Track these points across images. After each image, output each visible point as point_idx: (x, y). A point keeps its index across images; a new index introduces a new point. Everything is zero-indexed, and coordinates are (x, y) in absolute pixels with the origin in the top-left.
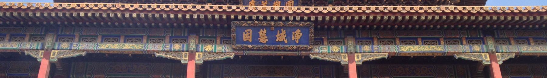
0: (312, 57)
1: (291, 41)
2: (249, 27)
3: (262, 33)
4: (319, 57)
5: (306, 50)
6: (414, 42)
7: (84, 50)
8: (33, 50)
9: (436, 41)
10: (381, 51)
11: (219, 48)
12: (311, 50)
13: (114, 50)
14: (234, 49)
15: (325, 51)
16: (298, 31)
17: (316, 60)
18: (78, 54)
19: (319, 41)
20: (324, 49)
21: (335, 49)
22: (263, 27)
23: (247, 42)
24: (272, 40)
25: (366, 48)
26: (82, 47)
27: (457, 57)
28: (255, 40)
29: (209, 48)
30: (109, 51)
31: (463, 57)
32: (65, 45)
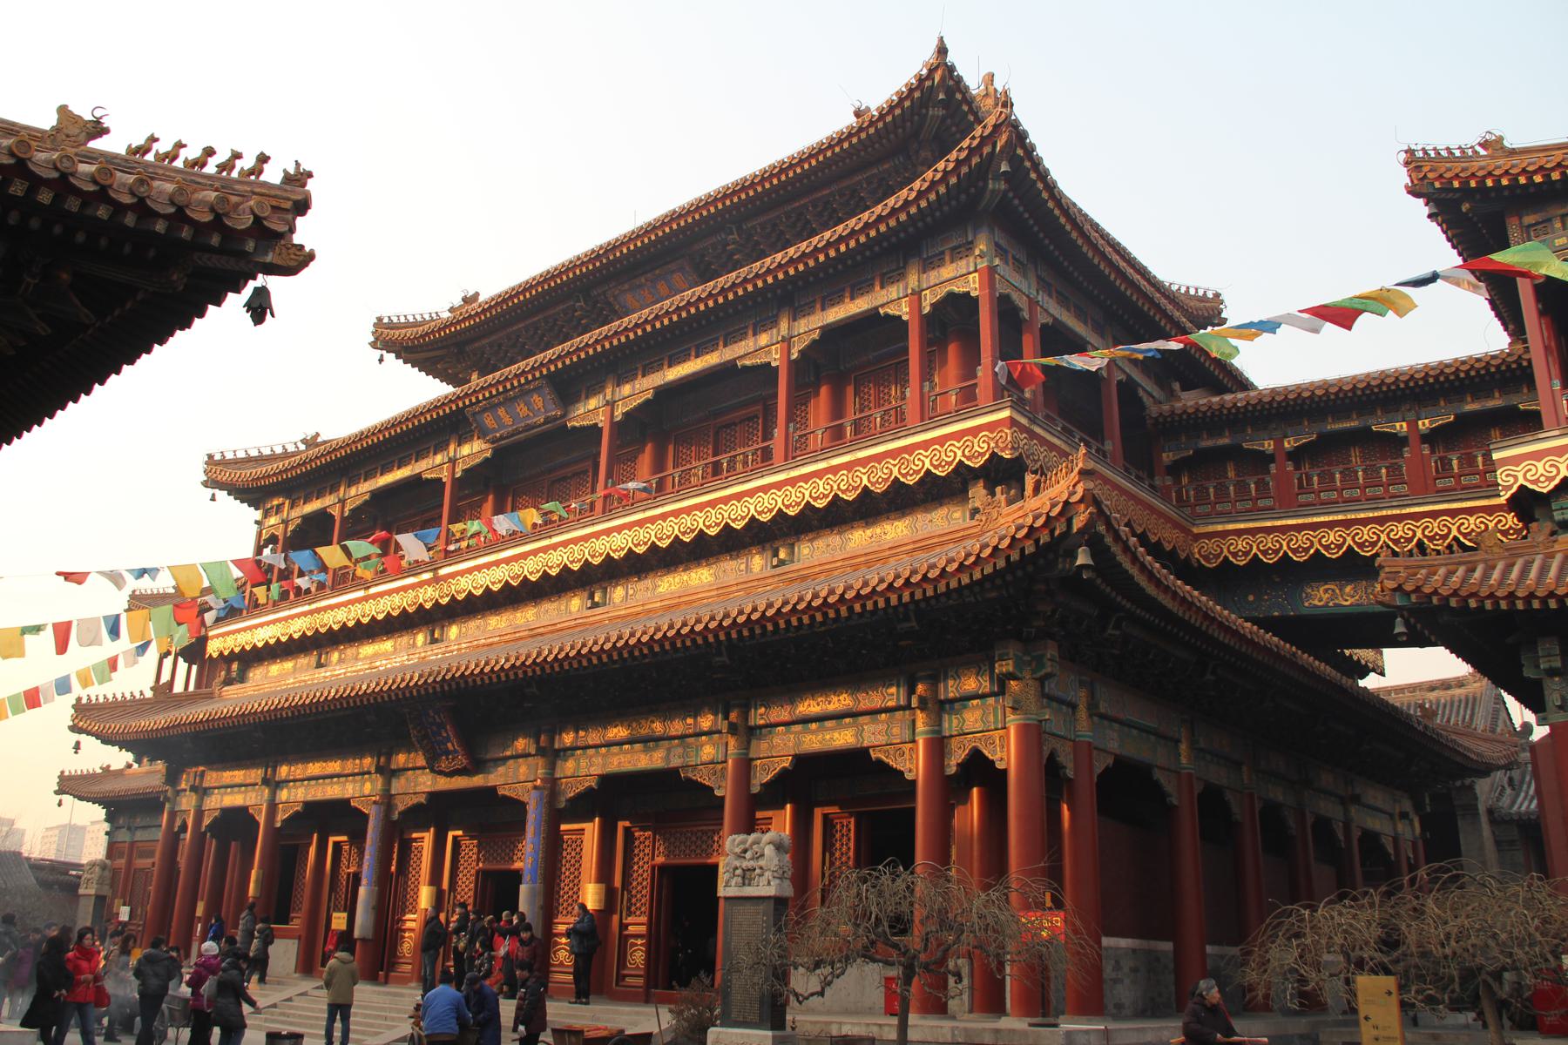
1: (537, 410)
2: (485, 410)
5: (555, 418)
6: (682, 358)
9: (710, 347)
10: (635, 392)
16: (535, 396)
17: (574, 428)
20: (581, 409)
22: (499, 404)
23: (494, 430)
24: (515, 417)
25: (627, 389)
28: (502, 426)
29: (466, 450)
31: (748, 362)
32: (353, 491)
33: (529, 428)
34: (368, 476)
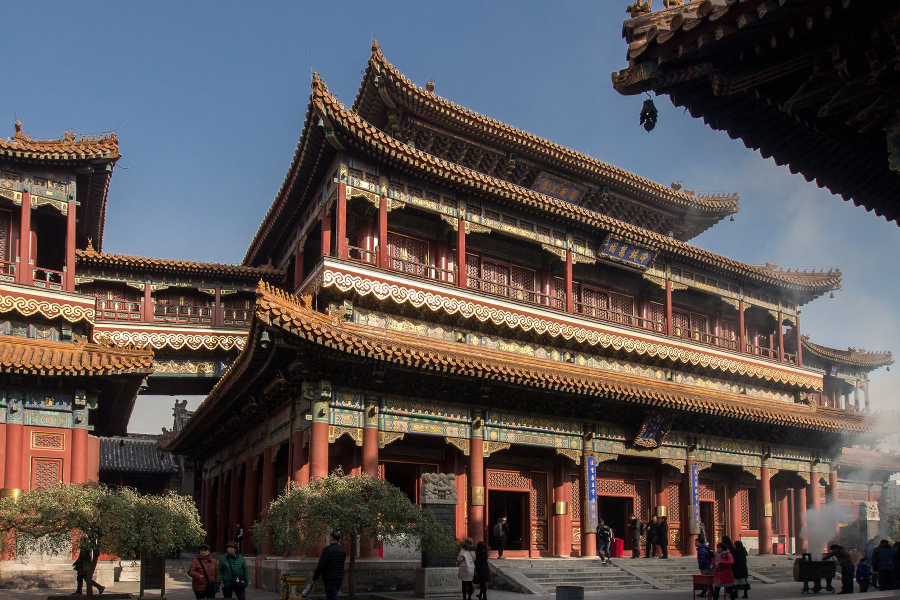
0: (645, 276)
1: (636, 260)
3: (624, 248)
4: (649, 278)
7: (489, 228)
8: (449, 216)
11: (588, 252)
12: (644, 270)
13: (513, 234)
14: (598, 256)
15: (655, 275)
17: (646, 279)
18: (485, 230)
19: (649, 264)
20: (652, 271)
21: (660, 273)
23: (611, 253)
24: (627, 256)
26: (492, 224)
27: (723, 299)
30: (508, 233)
33: (627, 264)
34: (496, 217)
